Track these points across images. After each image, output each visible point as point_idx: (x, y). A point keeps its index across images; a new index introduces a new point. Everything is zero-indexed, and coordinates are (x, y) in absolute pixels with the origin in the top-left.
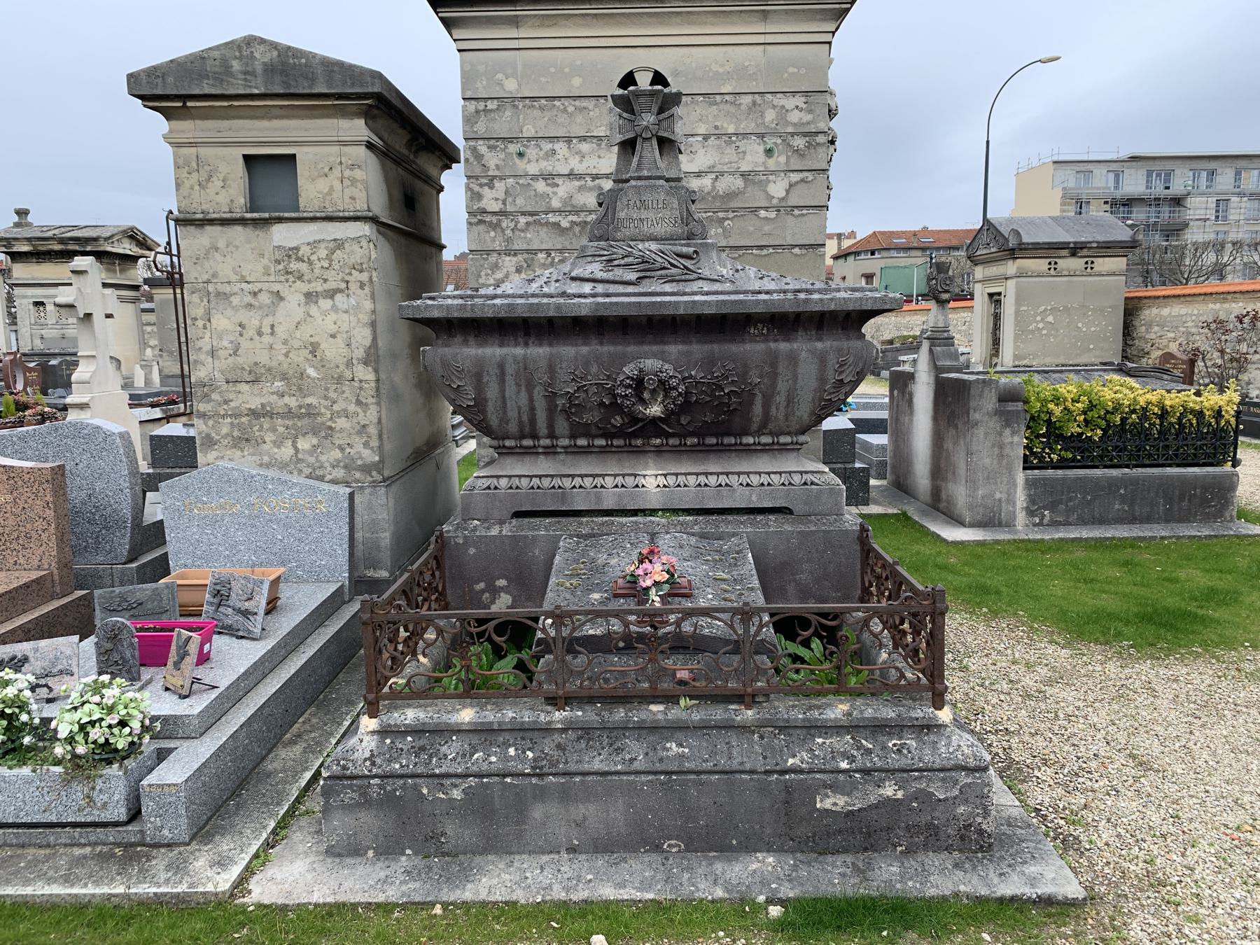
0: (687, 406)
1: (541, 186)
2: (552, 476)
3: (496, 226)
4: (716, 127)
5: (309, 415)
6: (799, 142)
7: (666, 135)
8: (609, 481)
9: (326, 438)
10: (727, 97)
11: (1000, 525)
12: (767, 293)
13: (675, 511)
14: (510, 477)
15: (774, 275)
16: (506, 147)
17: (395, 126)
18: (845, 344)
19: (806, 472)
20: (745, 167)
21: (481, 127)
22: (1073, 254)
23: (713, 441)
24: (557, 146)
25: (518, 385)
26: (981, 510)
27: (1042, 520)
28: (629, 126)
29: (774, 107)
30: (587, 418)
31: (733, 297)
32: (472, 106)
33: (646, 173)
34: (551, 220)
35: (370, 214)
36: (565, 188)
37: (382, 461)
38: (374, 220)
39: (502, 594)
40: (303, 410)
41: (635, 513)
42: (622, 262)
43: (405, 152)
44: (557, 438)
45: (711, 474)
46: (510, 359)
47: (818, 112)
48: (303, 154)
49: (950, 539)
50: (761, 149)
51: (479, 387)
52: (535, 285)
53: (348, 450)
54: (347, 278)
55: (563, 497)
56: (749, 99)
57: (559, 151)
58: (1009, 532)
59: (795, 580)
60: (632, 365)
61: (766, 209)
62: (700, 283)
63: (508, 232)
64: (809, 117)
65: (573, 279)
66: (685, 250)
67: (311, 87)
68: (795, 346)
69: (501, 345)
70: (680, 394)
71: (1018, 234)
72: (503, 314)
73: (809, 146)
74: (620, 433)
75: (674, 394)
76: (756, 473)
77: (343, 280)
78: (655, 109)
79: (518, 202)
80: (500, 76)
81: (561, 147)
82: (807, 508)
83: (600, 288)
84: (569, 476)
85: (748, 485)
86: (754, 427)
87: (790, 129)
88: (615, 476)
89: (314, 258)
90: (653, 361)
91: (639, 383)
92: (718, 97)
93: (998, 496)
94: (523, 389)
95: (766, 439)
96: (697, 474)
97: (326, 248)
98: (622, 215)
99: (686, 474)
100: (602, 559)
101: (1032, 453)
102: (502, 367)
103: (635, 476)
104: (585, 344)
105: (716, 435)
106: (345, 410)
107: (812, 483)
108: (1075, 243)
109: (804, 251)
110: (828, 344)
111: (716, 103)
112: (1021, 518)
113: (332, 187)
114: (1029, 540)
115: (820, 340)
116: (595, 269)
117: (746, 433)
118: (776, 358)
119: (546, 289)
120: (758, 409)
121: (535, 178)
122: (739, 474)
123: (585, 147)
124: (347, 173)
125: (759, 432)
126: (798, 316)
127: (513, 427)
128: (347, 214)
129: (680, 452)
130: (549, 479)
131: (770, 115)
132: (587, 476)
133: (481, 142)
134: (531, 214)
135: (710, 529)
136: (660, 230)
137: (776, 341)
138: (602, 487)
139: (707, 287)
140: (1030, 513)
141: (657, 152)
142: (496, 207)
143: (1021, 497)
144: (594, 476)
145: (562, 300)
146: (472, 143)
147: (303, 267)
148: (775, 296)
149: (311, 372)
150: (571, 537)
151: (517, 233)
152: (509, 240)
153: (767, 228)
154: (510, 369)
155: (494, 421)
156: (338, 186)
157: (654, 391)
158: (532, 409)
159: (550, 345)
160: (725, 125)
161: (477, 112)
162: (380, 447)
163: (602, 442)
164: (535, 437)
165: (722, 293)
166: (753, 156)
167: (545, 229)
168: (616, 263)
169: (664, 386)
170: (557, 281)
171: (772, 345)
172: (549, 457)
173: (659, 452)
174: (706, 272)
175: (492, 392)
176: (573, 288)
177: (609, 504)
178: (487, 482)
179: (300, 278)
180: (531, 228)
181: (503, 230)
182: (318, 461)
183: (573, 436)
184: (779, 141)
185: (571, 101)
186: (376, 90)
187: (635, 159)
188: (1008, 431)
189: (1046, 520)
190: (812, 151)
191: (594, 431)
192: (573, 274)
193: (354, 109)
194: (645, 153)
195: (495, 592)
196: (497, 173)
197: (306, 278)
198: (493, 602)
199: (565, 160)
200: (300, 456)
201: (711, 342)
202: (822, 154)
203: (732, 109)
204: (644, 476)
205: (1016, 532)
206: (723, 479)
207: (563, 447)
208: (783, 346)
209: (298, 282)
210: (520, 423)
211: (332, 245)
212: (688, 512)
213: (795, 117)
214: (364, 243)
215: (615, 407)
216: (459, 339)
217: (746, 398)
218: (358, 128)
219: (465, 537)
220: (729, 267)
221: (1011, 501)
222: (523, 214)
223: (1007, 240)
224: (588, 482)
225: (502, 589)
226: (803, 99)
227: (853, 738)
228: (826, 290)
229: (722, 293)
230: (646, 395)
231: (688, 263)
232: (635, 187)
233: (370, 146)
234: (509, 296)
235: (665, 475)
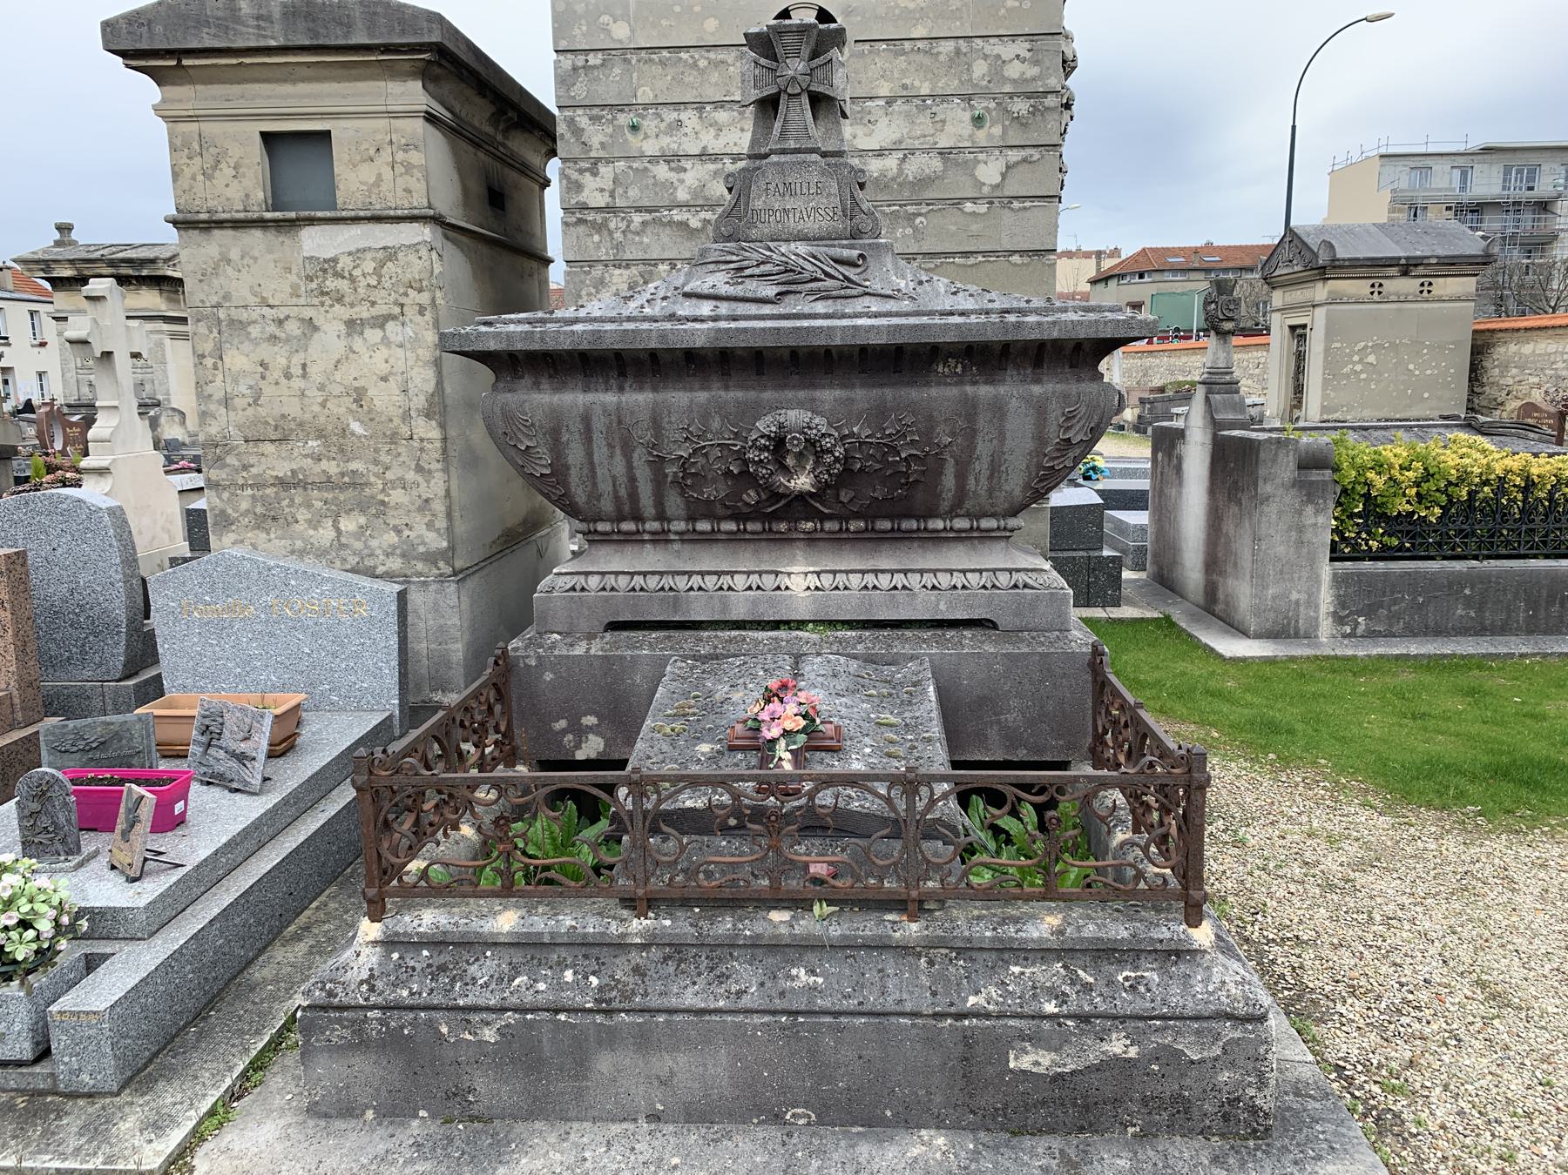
0: (848, 475)
1: (662, 171)
2: (661, 573)
3: (600, 228)
4: (905, 87)
5: (353, 485)
6: (1021, 106)
7: (820, 89)
8: (740, 581)
9: (376, 516)
10: (920, 44)
11: (1297, 635)
12: (962, 314)
13: (832, 624)
14: (603, 574)
15: (973, 288)
16: (614, 118)
17: (469, 92)
18: (1074, 388)
19: (1018, 570)
20: (944, 143)
21: (580, 91)
22: (1405, 274)
23: (887, 525)
24: (684, 116)
25: (610, 446)
26: (1272, 615)
28: (769, 77)
29: (986, 57)
30: (709, 492)
31: (912, 320)
32: (567, 61)
33: (792, 144)
34: (676, 218)
35: (431, 212)
36: (695, 174)
37: (452, 548)
38: (437, 220)
39: (591, 736)
40: (346, 479)
41: (776, 625)
42: (757, 271)
43: (489, 130)
44: (669, 521)
45: (883, 571)
46: (598, 410)
47: (1047, 64)
48: (336, 127)
49: (1228, 654)
50: (967, 116)
51: (557, 448)
52: (632, 304)
53: (407, 533)
54: (402, 300)
55: (676, 604)
56: (949, 46)
57: (687, 122)
58: (1309, 646)
59: (999, 722)
60: (769, 418)
61: (974, 200)
62: (867, 300)
63: (618, 235)
64: (1035, 71)
65: (687, 295)
66: (846, 253)
67: (346, 36)
68: (1002, 390)
69: (586, 390)
70: (837, 460)
71: (1331, 246)
72: (585, 346)
73: (1034, 111)
74: (755, 513)
75: (829, 459)
77: (396, 303)
78: (806, 52)
79: (631, 193)
80: (605, 18)
81: (689, 117)
83: (724, 308)
85: (934, 587)
86: (945, 506)
87: (1008, 89)
88: (749, 573)
89: (355, 273)
90: (798, 412)
91: (778, 444)
92: (907, 45)
93: (1294, 596)
94: (618, 451)
95: (961, 524)
96: (863, 572)
97: (374, 259)
98: (758, 204)
99: (847, 572)
100: (721, 691)
101: (1343, 539)
102: (586, 420)
103: (777, 573)
104: (703, 389)
105: (891, 517)
106: (401, 479)
107: (1025, 586)
108: (1407, 258)
109: (1026, 260)
110: (1048, 388)
111: (904, 53)
112: (1326, 627)
113: (379, 175)
114: (1336, 657)
115: (1038, 381)
116: (718, 281)
117: (932, 514)
118: (974, 407)
119: (647, 310)
120: (949, 481)
121: (654, 160)
122: (921, 572)
123: (722, 116)
124: (400, 156)
125: (952, 513)
126: (1006, 347)
127: (607, 505)
128: (399, 212)
129: (840, 540)
130: (657, 577)
131: (980, 69)
132: (709, 573)
133: (580, 111)
134: (649, 210)
135: (879, 649)
136: (811, 226)
137: (974, 383)
138: (730, 588)
139: (875, 306)
140: (1339, 620)
141: (809, 114)
142: (600, 200)
143: (1326, 599)
144: (719, 574)
145: (668, 326)
146: (568, 113)
147: (343, 285)
148: (973, 319)
149: (356, 427)
150: (684, 658)
151: (630, 236)
152: (618, 247)
153: (974, 227)
154: (599, 424)
155: (580, 496)
156: (387, 174)
157: (800, 456)
158: (632, 479)
159: (655, 389)
160: (917, 83)
161: (575, 69)
162: (450, 529)
163: (730, 526)
164: (638, 518)
165: (898, 314)
166: (956, 127)
167: (668, 230)
168: (748, 272)
169: (813, 447)
170: (665, 298)
171: (969, 389)
172: (660, 547)
173: (811, 540)
174: (876, 286)
175: (575, 455)
176: (686, 308)
177: (739, 613)
178: (570, 581)
179: (340, 300)
180: (649, 230)
181: (611, 233)
182: (367, 547)
183: (691, 518)
184: (992, 105)
185: (703, 52)
186: (434, 40)
187: (778, 125)
188: (1310, 509)
189: (1361, 629)
190: (1039, 118)
191: (720, 511)
192: (686, 289)
193: (407, 66)
194: (792, 116)
195: (580, 733)
196: (602, 154)
197: (347, 300)
198: (578, 746)
199: (696, 135)
200: (343, 540)
201: (881, 385)
202: (1052, 123)
203: (927, 60)
204: (789, 574)
205: (1318, 645)
206: (899, 579)
207: (677, 533)
208: (984, 391)
209: (337, 306)
210: (617, 497)
211: (380, 255)
213: (1014, 70)
214: (424, 252)
215: (746, 477)
216: (527, 381)
217: (932, 463)
218: (412, 94)
219: (539, 657)
220: (910, 277)
221: (1312, 603)
222: (639, 209)
223: (1316, 255)
224: (710, 581)
225: (590, 729)
226: (1027, 45)
227: (1065, 967)
228: (1046, 310)
229: (898, 314)
230: (790, 461)
231: (851, 272)
232: (777, 164)
233: (430, 118)
234: (595, 320)
235: (818, 574)
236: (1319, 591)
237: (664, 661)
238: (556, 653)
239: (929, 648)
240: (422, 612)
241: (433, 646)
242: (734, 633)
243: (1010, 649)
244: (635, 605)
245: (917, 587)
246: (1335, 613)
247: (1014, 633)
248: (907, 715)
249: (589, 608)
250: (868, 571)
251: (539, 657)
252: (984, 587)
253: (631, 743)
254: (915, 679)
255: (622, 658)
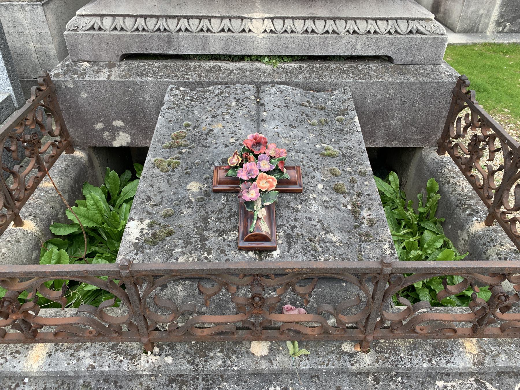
2: (157, 17)
8: (216, 25)
11: (477, 32)
13: (281, 58)
14: (114, 16)
19: (413, 19)
26: (468, 21)
27: (503, 29)
41: (241, 58)
45: (319, 18)
55: (170, 41)
58: (482, 37)
59: (385, 126)
76: (363, 19)
82: (407, 58)
84: (174, 17)
85: (354, 32)
88: (222, 18)
93: (481, 12)
96: (305, 19)
99: (293, 18)
100: (206, 120)
103: (242, 18)
107: (418, 32)
112: (491, 27)
114: (494, 44)
122: (346, 19)
130: (154, 20)
132: (193, 17)
135: (314, 79)
138: (208, 30)
140: (498, 24)
144: (200, 18)
150: (178, 85)
177: (215, 49)
178: (89, 22)
195: (114, 131)
198: (114, 139)
204: (251, 19)
205: (486, 37)
206: (330, 25)
212: (294, 58)
219: (75, 82)
221: (488, 16)
224: (194, 24)
225: (120, 129)
227: (477, 380)
235: (272, 19)
236: (493, 10)
237: (163, 87)
238: (86, 78)
239: (347, 78)
240: (25, 24)
241: (37, 46)
242: (213, 63)
243: (401, 79)
244: (140, 42)
245: (342, 31)
246: (498, 20)
247: (402, 68)
248: (342, 144)
249: (107, 44)
250: (308, 18)
251: (75, 82)
252: (389, 32)
253: (149, 136)
254: (342, 107)
255: (134, 83)
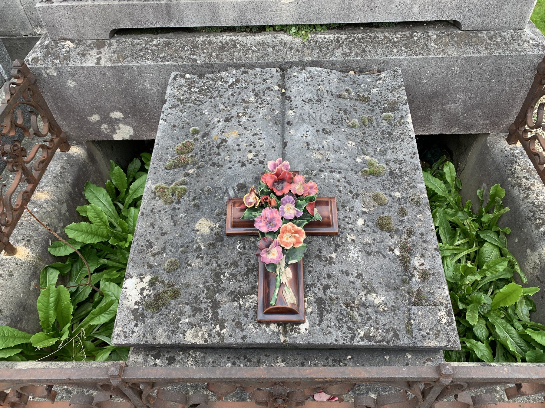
39: (121, 125)
41: (262, 29)
59: (443, 110)
82: (480, 22)
135: (355, 57)
195: (113, 124)
198: (114, 132)
212: (330, 27)
225: (119, 120)
238: (71, 64)
242: (226, 37)
243: (470, 52)
244: (132, 14)
247: (472, 36)
248: (390, 155)
249: (91, 17)
251: (57, 69)
253: (154, 128)
255: (130, 68)
